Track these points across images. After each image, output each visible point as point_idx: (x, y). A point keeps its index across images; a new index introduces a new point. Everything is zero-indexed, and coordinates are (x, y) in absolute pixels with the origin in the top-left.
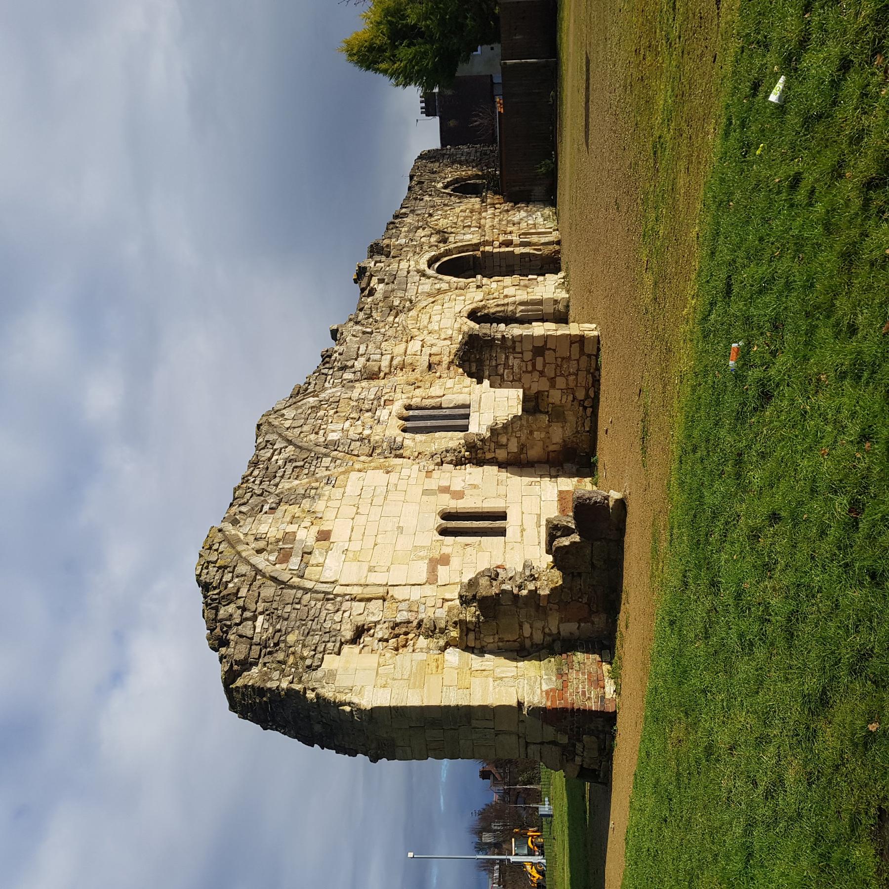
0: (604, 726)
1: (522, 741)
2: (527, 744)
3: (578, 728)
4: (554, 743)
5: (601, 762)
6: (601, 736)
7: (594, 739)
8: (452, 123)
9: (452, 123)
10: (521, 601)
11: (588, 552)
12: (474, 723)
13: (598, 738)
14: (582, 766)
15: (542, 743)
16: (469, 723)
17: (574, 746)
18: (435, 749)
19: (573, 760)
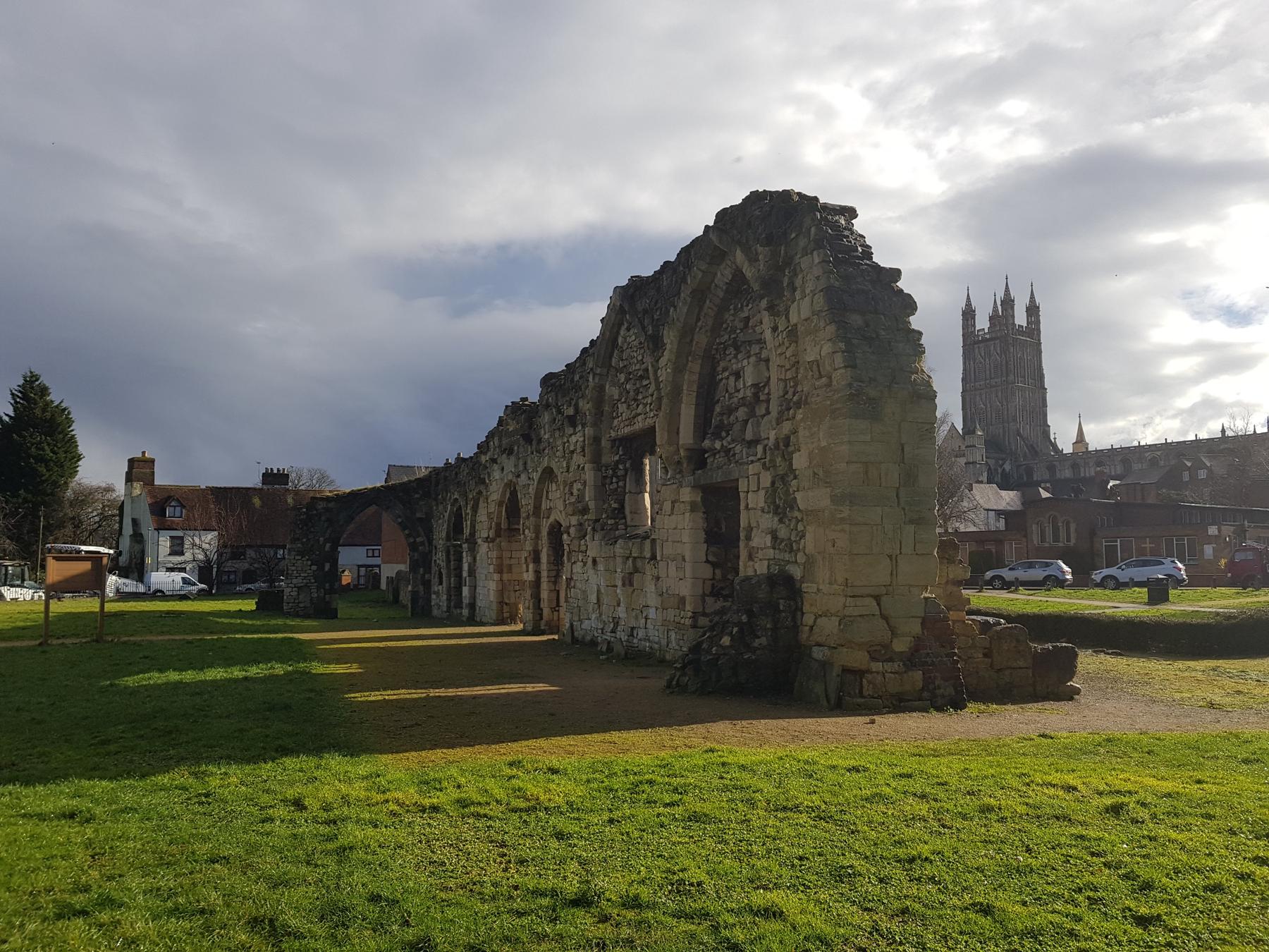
0: (943, 696)
1: (883, 590)
2: (877, 598)
3: (933, 664)
4: (894, 633)
5: (880, 697)
6: (925, 694)
7: (920, 685)
8: (257, 501)
9: (257, 501)
10: (955, 589)
11: (1021, 663)
12: (911, 528)
13: (923, 689)
14: (869, 671)
15: (885, 618)
16: (911, 522)
17: (891, 660)
18: (866, 472)
19: (873, 659)
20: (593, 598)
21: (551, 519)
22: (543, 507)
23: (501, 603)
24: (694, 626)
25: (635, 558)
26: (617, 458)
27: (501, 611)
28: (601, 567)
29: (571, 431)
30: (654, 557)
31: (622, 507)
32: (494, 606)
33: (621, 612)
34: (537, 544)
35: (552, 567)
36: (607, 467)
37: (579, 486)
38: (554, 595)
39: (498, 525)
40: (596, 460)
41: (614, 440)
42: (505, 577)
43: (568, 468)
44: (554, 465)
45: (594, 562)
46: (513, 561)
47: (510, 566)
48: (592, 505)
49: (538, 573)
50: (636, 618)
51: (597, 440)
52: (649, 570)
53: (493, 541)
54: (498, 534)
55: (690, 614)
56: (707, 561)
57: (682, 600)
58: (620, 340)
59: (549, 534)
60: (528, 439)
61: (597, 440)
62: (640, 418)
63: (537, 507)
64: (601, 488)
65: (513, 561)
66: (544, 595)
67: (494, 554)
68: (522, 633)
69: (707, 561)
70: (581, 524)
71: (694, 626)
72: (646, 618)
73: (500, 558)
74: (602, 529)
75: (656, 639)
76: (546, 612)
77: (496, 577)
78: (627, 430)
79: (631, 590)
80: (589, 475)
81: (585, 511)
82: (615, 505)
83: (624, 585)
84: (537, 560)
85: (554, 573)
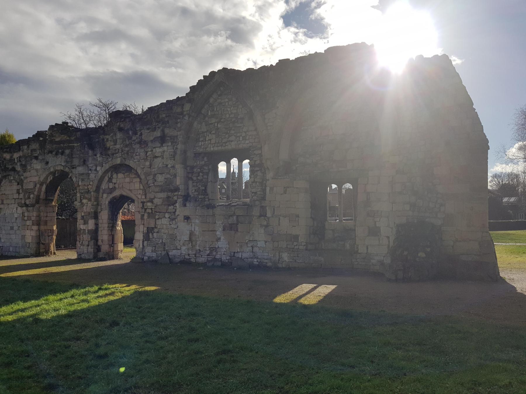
20: (186, 238)
21: (117, 193)
22: (104, 186)
23: (39, 243)
24: (306, 250)
25: (238, 216)
26: (203, 163)
27: (38, 248)
29: (159, 145)
30: (263, 215)
31: (205, 190)
32: (33, 246)
33: (223, 244)
34: (97, 208)
35: (111, 222)
36: (192, 168)
37: (168, 176)
38: (111, 237)
39: (38, 196)
40: (184, 162)
41: (200, 154)
42: (42, 228)
43: (151, 165)
44: (131, 164)
46: (48, 219)
47: (46, 223)
48: (182, 187)
49: (97, 225)
50: (241, 247)
51: (185, 152)
53: (33, 206)
54: (38, 201)
55: (304, 244)
56: (311, 218)
57: (296, 237)
58: (211, 100)
59: (110, 202)
60: (92, 147)
61: (185, 152)
62: (233, 143)
63: (98, 188)
64: (188, 178)
65: (48, 219)
66: (104, 236)
67: (35, 214)
68: (80, 260)
69: (311, 218)
70: (168, 197)
71: (306, 250)
72: (252, 247)
73: (38, 216)
74: (196, 201)
75: (265, 257)
76: (105, 248)
77: (35, 228)
78: (216, 149)
79: (233, 232)
80: (180, 170)
81: (177, 189)
82: (203, 188)
83: (224, 230)
84: (96, 216)
85: (111, 225)
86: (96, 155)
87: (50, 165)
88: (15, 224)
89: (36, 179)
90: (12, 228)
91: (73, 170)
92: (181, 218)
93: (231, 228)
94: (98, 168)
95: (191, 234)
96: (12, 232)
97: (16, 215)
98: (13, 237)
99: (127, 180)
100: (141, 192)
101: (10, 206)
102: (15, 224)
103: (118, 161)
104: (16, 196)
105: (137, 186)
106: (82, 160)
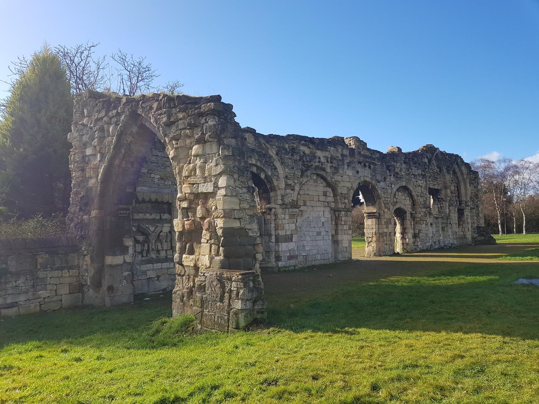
21: (397, 206)
28: (434, 226)
33: (441, 238)
44: (411, 187)
45: (431, 224)
52: (450, 226)
86: (391, 176)
87: (360, 174)
88: (322, 229)
89: (349, 185)
90: (319, 234)
91: (378, 184)
92: (429, 224)
93: (443, 229)
94: (393, 186)
95: (433, 233)
96: (318, 238)
97: (323, 220)
98: (321, 243)
99: (403, 197)
100: (410, 206)
101: (315, 209)
102: (322, 229)
103: (404, 184)
104: (322, 198)
105: (408, 202)
106: (383, 177)
